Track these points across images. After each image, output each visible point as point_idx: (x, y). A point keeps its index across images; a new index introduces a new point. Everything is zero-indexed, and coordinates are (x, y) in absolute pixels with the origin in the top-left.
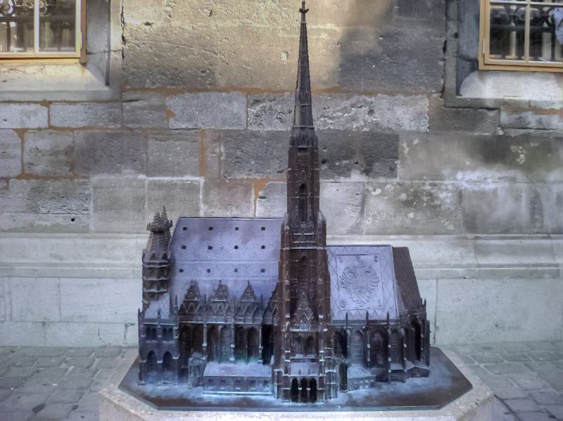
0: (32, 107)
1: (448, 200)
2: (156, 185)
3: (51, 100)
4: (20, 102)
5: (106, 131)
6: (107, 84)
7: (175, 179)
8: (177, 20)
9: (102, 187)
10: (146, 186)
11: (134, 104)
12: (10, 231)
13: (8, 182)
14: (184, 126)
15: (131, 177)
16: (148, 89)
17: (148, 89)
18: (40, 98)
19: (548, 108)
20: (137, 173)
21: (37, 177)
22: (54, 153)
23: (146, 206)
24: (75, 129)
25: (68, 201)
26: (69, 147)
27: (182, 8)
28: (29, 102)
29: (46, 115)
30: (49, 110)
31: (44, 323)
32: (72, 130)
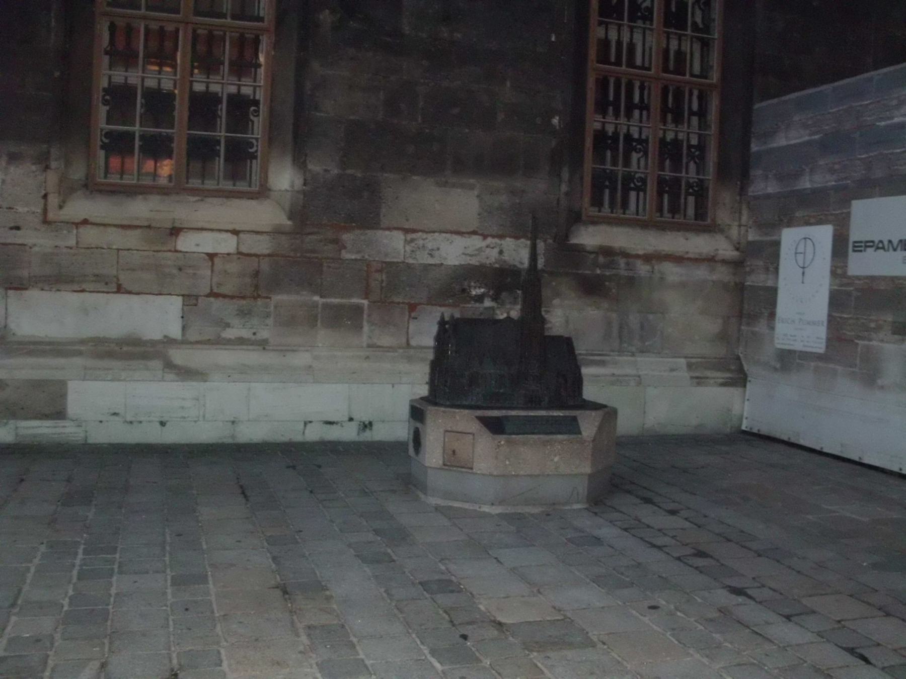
1: (557, 324)
12: (198, 342)
13: (197, 300)
14: (353, 257)
19: (634, 253)
31: (233, 422)
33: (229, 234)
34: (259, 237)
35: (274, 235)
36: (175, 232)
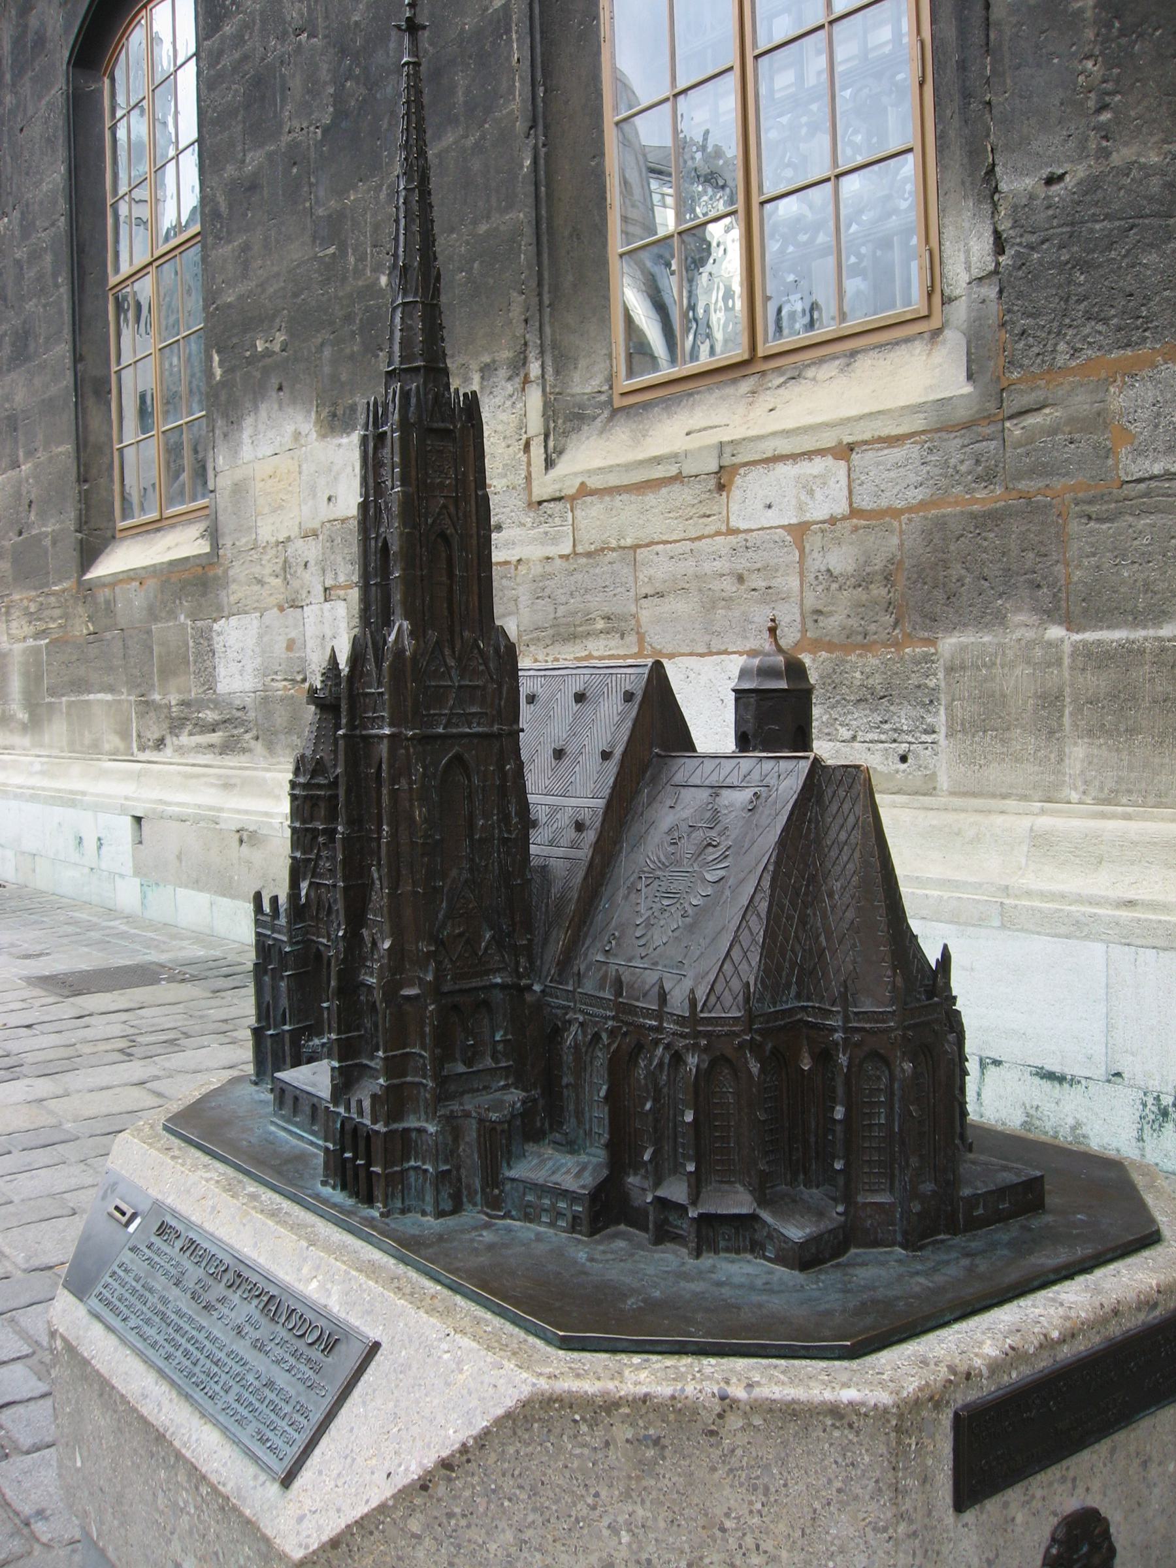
0: (818, 465)
2: (1089, 655)
3: (850, 439)
4: (794, 457)
5: (969, 508)
6: (970, 377)
7: (1140, 634)
8: (1126, 144)
9: (963, 668)
10: (1067, 661)
11: (1031, 420)
14: (1157, 469)
15: (1030, 634)
16: (1064, 370)
17: (1064, 370)
18: (828, 440)
20: (1042, 622)
21: (830, 647)
22: (863, 581)
23: (1067, 720)
24: (901, 512)
25: (892, 708)
26: (891, 561)
27: (1139, 103)
28: (809, 455)
29: (844, 482)
30: (849, 469)
32: (896, 513)
33: (829, 460)
34: (896, 454)
35: (931, 440)
36: (722, 479)
